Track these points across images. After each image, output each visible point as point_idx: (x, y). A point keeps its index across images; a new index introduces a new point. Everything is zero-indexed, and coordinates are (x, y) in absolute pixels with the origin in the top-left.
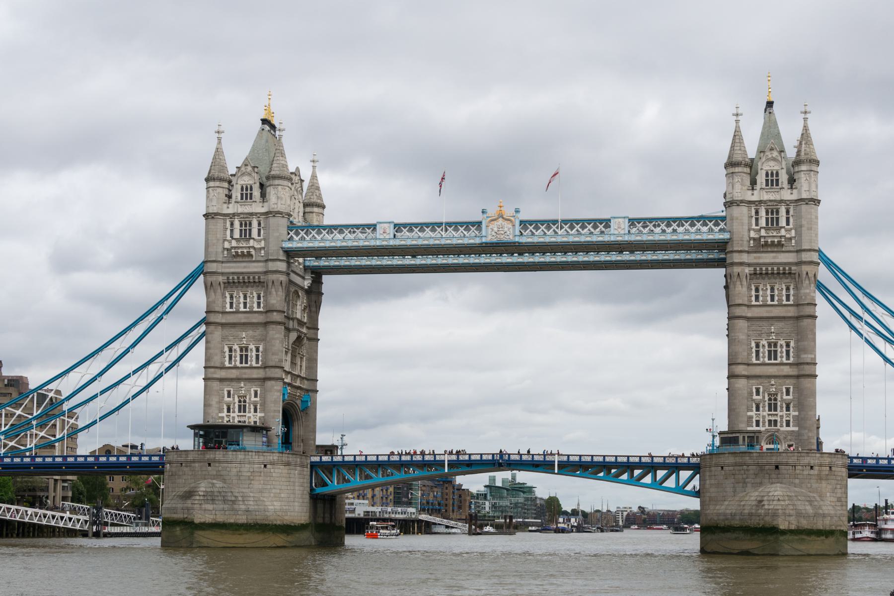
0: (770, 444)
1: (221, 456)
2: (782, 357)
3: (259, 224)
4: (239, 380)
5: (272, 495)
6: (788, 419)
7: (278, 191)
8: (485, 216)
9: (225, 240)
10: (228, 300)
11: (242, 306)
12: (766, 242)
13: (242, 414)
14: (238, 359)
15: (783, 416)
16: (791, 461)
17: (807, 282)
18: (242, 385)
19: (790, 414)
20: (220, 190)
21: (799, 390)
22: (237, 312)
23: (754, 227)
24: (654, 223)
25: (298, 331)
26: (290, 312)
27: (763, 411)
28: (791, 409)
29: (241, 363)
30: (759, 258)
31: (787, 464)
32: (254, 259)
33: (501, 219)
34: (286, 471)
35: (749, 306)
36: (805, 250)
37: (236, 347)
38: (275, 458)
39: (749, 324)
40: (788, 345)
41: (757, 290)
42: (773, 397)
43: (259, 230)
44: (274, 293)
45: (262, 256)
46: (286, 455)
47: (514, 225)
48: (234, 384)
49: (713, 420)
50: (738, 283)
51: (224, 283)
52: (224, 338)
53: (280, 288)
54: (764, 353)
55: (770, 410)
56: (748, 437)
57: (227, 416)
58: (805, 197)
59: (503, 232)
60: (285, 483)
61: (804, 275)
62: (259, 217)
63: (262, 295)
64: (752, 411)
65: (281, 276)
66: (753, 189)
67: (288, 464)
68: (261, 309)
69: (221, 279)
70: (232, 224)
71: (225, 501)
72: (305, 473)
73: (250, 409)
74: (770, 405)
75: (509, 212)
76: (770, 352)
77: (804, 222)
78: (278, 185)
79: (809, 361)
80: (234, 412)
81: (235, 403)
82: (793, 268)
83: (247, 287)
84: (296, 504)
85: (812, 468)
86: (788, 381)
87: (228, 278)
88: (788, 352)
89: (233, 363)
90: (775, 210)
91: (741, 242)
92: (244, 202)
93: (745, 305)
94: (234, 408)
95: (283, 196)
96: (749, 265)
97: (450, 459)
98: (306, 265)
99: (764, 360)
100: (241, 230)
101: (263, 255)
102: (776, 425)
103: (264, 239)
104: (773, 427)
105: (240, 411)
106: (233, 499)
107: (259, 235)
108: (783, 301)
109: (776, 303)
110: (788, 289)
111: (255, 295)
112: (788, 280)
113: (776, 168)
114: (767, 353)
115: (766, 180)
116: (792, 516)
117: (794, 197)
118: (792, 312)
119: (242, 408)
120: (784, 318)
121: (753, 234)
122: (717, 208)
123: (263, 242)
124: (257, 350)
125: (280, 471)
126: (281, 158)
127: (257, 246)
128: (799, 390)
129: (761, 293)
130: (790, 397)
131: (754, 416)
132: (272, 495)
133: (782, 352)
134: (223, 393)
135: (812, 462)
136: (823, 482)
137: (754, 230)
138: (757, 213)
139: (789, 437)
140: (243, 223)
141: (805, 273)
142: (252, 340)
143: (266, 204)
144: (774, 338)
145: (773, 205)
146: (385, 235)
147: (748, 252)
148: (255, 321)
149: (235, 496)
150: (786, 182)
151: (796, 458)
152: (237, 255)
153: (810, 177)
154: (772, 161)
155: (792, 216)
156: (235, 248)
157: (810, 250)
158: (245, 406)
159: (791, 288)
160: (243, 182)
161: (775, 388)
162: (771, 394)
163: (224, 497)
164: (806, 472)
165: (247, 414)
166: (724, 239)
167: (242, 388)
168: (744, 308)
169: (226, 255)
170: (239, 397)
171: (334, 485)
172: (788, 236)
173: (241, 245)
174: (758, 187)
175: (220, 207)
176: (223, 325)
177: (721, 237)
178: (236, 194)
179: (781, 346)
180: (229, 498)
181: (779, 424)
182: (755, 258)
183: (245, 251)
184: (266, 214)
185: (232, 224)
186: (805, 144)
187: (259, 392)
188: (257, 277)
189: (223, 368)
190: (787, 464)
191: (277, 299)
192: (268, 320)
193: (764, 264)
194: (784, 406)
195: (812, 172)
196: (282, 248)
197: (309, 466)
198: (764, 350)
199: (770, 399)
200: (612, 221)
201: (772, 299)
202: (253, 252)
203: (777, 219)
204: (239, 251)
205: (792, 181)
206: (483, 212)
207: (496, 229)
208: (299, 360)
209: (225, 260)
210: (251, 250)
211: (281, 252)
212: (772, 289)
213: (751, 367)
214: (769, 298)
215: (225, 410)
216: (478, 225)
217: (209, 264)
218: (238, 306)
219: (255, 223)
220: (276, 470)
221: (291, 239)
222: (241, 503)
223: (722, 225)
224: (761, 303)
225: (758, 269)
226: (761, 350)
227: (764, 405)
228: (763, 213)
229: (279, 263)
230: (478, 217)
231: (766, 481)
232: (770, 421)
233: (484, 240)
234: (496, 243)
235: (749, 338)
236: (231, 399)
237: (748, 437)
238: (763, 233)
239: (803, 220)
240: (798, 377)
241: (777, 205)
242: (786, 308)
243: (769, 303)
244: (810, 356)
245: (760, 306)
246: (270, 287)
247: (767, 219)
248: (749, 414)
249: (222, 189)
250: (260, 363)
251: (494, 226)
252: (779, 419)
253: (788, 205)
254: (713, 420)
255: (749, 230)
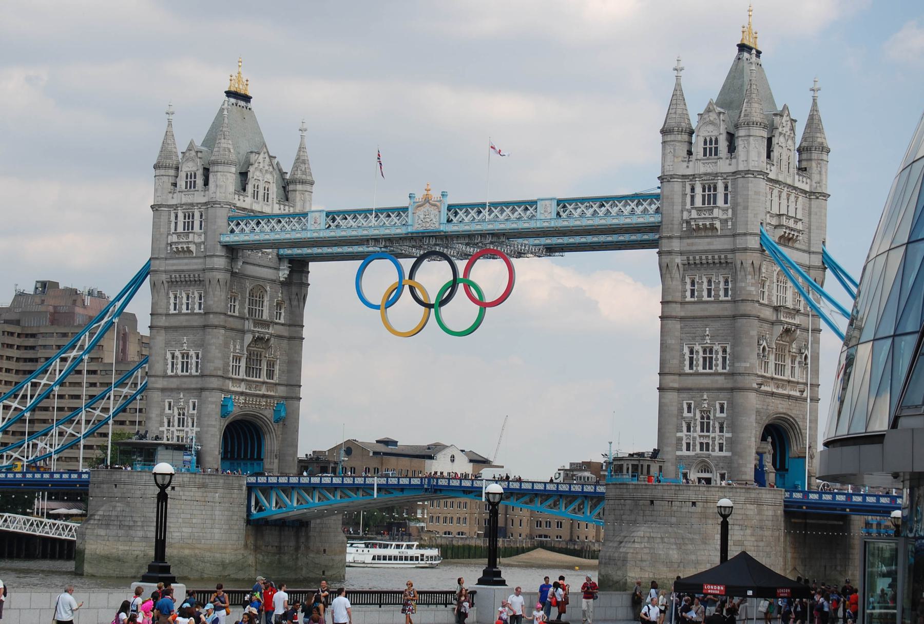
0: (702, 472)
1: (127, 476)
2: (717, 365)
3: (201, 216)
4: (178, 390)
5: (180, 520)
6: (721, 441)
7: (217, 178)
8: (412, 201)
9: (169, 234)
10: (172, 301)
11: (184, 307)
12: (697, 225)
13: (181, 428)
14: (180, 366)
15: (715, 438)
16: (666, 495)
17: (743, 273)
18: (182, 396)
19: (723, 436)
20: (165, 179)
21: (732, 404)
22: (180, 314)
23: (688, 206)
24: (585, 204)
25: (253, 332)
26: (246, 311)
27: (693, 432)
28: (725, 429)
29: (182, 371)
30: (692, 244)
31: (662, 499)
32: (194, 255)
33: (428, 204)
34: (200, 494)
35: (683, 303)
36: (739, 234)
37: (177, 353)
38: (185, 479)
39: (682, 325)
40: (724, 351)
41: (693, 284)
42: (705, 415)
43: (201, 222)
44: (211, 293)
45: (202, 252)
46: (201, 476)
47: (440, 212)
48: (175, 394)
49: (611, 443)
50: (668, 276)
51: (168, 282)
52: (168, 344)
53: (218, 286)
54: (697, 360)
55: (702, 431)
56: (633, 465)
57: (167, 430)
58: (743, 169)
59: (428, 220)
60: (197, 507)
61: (739, 266)
62: (200, 208)
63: (202, 295)
64: (682, 431)
65: (217, 273)
66: (689, 161)
67: (203, 486)
68: (202, 311)
69: (164, 277)
70: (176, 217)
71: (120, 527)
72: (235, 496)
73: (187, 423)
74: (702, 424)
75: (435, 195)
76: (705, 359)
77: (740, 200)
78: (217, 172)
79: (742, 371)
80: (173, 426)
81: (174, 416)
82: (729, 256)
83: (189, 286)
84: (216, 531)
85: (694, 504)
86: (722, 395)
87: (171, 276)
88: (724, 359)
89: (175, 371)
90: (712, 185)
91: (670, 226)
92: (188, 191)
93: (676, 302)
94: (174, 421)
95: (222, 183)
96: (681, 253)
97: (380, 483)
98: (280, 253)
99: (697, 369)
100: (185, 222)
101: (202, 250)
102: (708, 450)
103: (205, 233)
104: (705, 452)
105: (179, 426)
106: (131, 524)
107: (201, 229)
108: (720, 296)
109: (712, 299)
110: (726, 282)
111: (197, 295)
112: (726, 271)
113: (715, 133)
114: (701, 360)
115: (704, 148)
116: (645, 561)
117: (732, 169)
118: (728, 310)
119: (181, 422)
120: (719, 317)
121: (685, 216)
122: (651, 185)
123: (203, 235)
124: (197, 358)
125: (192, 494)
126: (223, 141)
127: (197, 240)
128: (732, 404)
129: (696, 287)
130: (724, 415)
131: (684, 438)
132: (180, 520)
133: (717, 359)
134: (164, 405)
135: (693, 498)
136: (710, 522)
137: (687, 210)
138: (693, 190)
139: (721, 464)
140: (187, 214)
141: (739, 263)
142: (192, 345)
143: (207, 192)
144: (709, 342)
145: (709, 180)
146: (316, 225)
147: (681, 238)
148: (195, 324)
149: (134, 522)
150: (726, 150)
151: (673, 492)
152: (178, 252)
153: (749, 143)
154: (711, 125)
155: (730, 192)
156: (175, 243)
157: (745, 234)
158: (183, 419)
159: (730, 280)
160: (187, 169)
161: (708, 404)
162: (704, 411)
163: (120, 521)
164: (684, 510)
165: (185, 429)
166: (654, 223)
167: (181, 399)
168: (674, 305)
169: (169, 251)
170: (178, 409)
171: (271, 509)
172: (725, 217)
173: (182, 240)
174: (693, 157)
175: (165, 197)
176: (166, 328)
177: (652, 220)
178: (182, 183)
179: (717, 353)
180: (127, 524)
181: (711, 448)
182: (688, 245)
183: (185, 246)
184: (206, 204)
185: (176, 217)
186: (747, 103)
187: (196, 404)
188: (197, 276)
189: (165, 376)
190: (662, 499)
191: (218, 298)
192: (206, 323)
193: (697, 252)
194: (717, 425)
195: (751, 138)
196: (220, 242)
197: (244, 488)
198: (697, 357)
199: (702, 418)
200: (538, 203)
201: (709, 295)
202: (193, 248)
203: (715, 196)
204: (179, 247)
205: (732, 148)
206: (410, 197)
207: (422, 217)
208: (266, 363)
209: (168, 256)
210: (190, 246)
211: (219, 247)
212: (709, 282)
213: (683, 378)
214: (705, 293)
215: (166, 424)
216: (405, 210)
217: (152, 262)
218: (181, 308)
219: (197, 215)
220: (187, 493)
221: (232, 231)
222: (139, 529)
223: (658, 204)
224: (696, 299)
225: (691, 258)
226: (695, 357)
227: (695, 424)
228: (699, 190)
229: (216, 259)
230: (404, 202)
231: (640, 518)
232: (701, 444)
233: (410, 229)
234: (422, 233)
235: (682, 342)
236: (171, 412)
237: (633, 465)
238: (694, 214)
239: (739, 197)
240: (732, 390)
241: (714, 179)
242: (722, 305)
243: (705, 298)
244: (744, 365)
245: (694, 303)
246: (207, 287)
247: (704, 196)
248: (679, 434)
249: (167, 177)
250: (199, 371)
251: (421, 213)
252: (711, 443)
253: (725, 179)
254: (611, 443)
255: (682, 211)
